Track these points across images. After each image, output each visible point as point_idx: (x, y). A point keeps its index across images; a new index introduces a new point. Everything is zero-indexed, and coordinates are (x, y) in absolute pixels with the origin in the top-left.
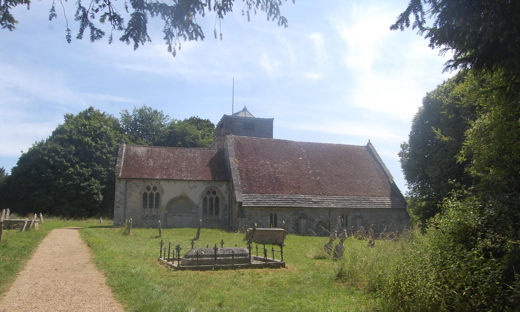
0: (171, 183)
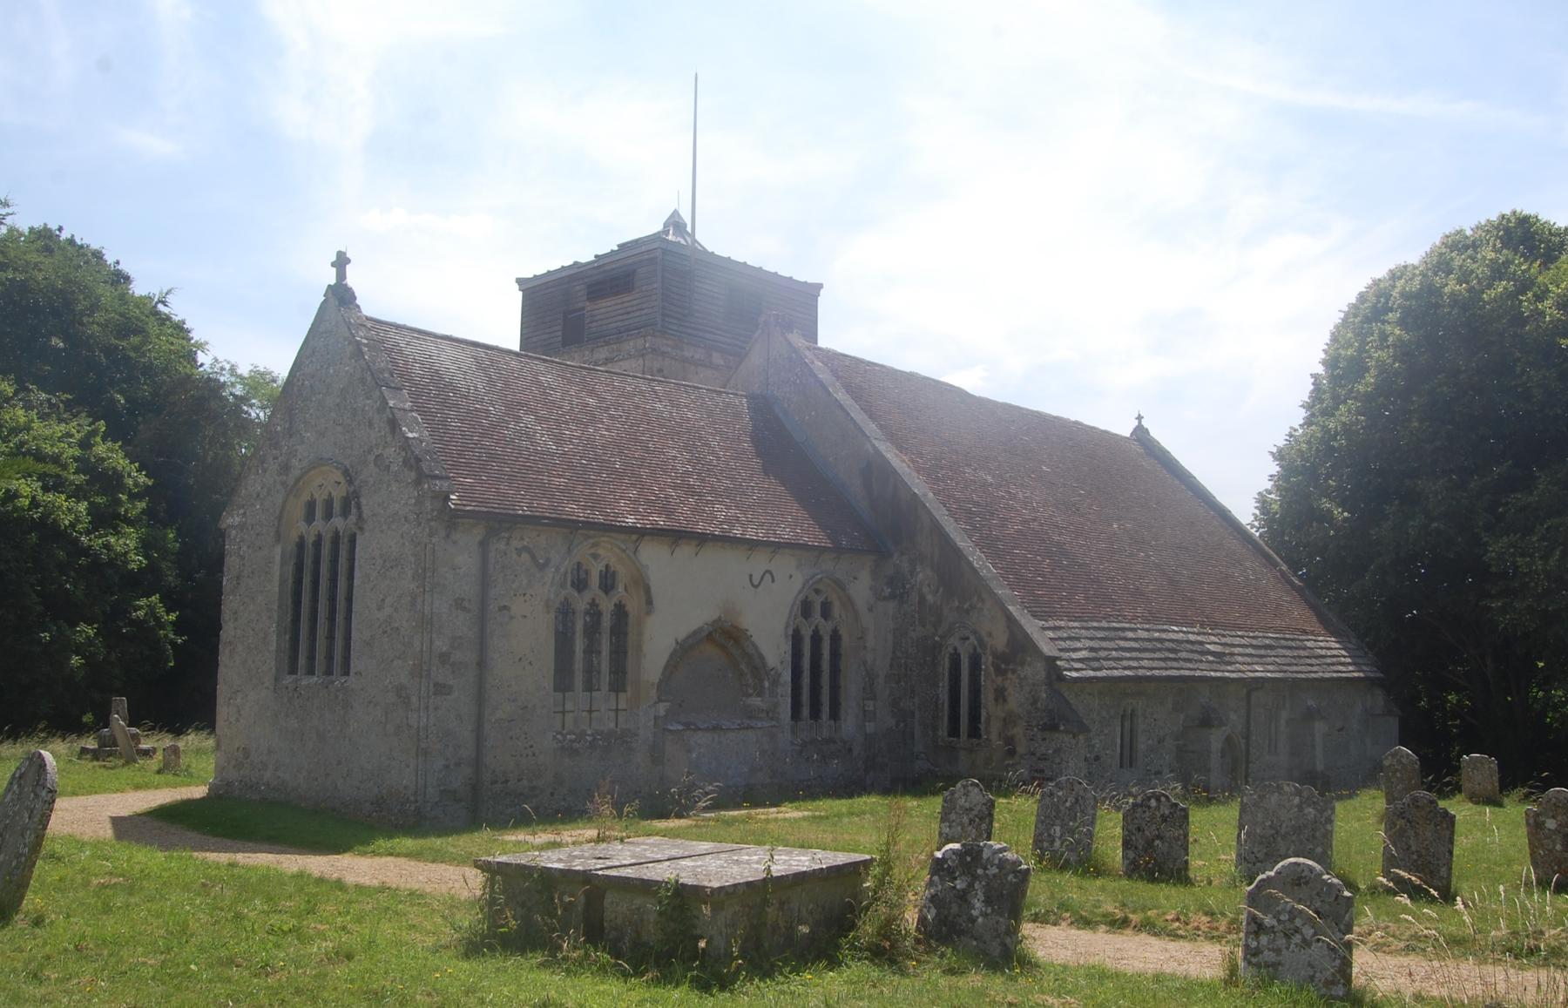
0: (685, 550)
